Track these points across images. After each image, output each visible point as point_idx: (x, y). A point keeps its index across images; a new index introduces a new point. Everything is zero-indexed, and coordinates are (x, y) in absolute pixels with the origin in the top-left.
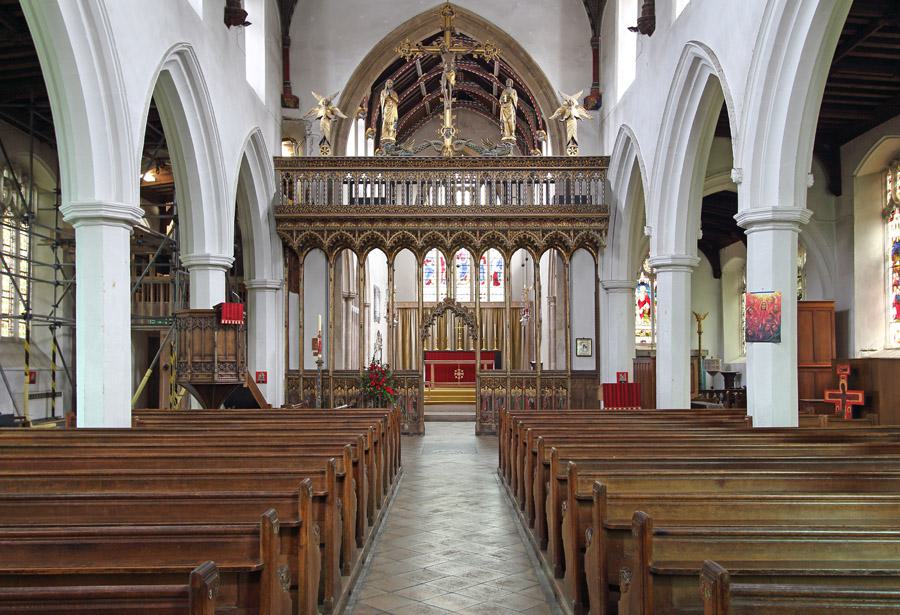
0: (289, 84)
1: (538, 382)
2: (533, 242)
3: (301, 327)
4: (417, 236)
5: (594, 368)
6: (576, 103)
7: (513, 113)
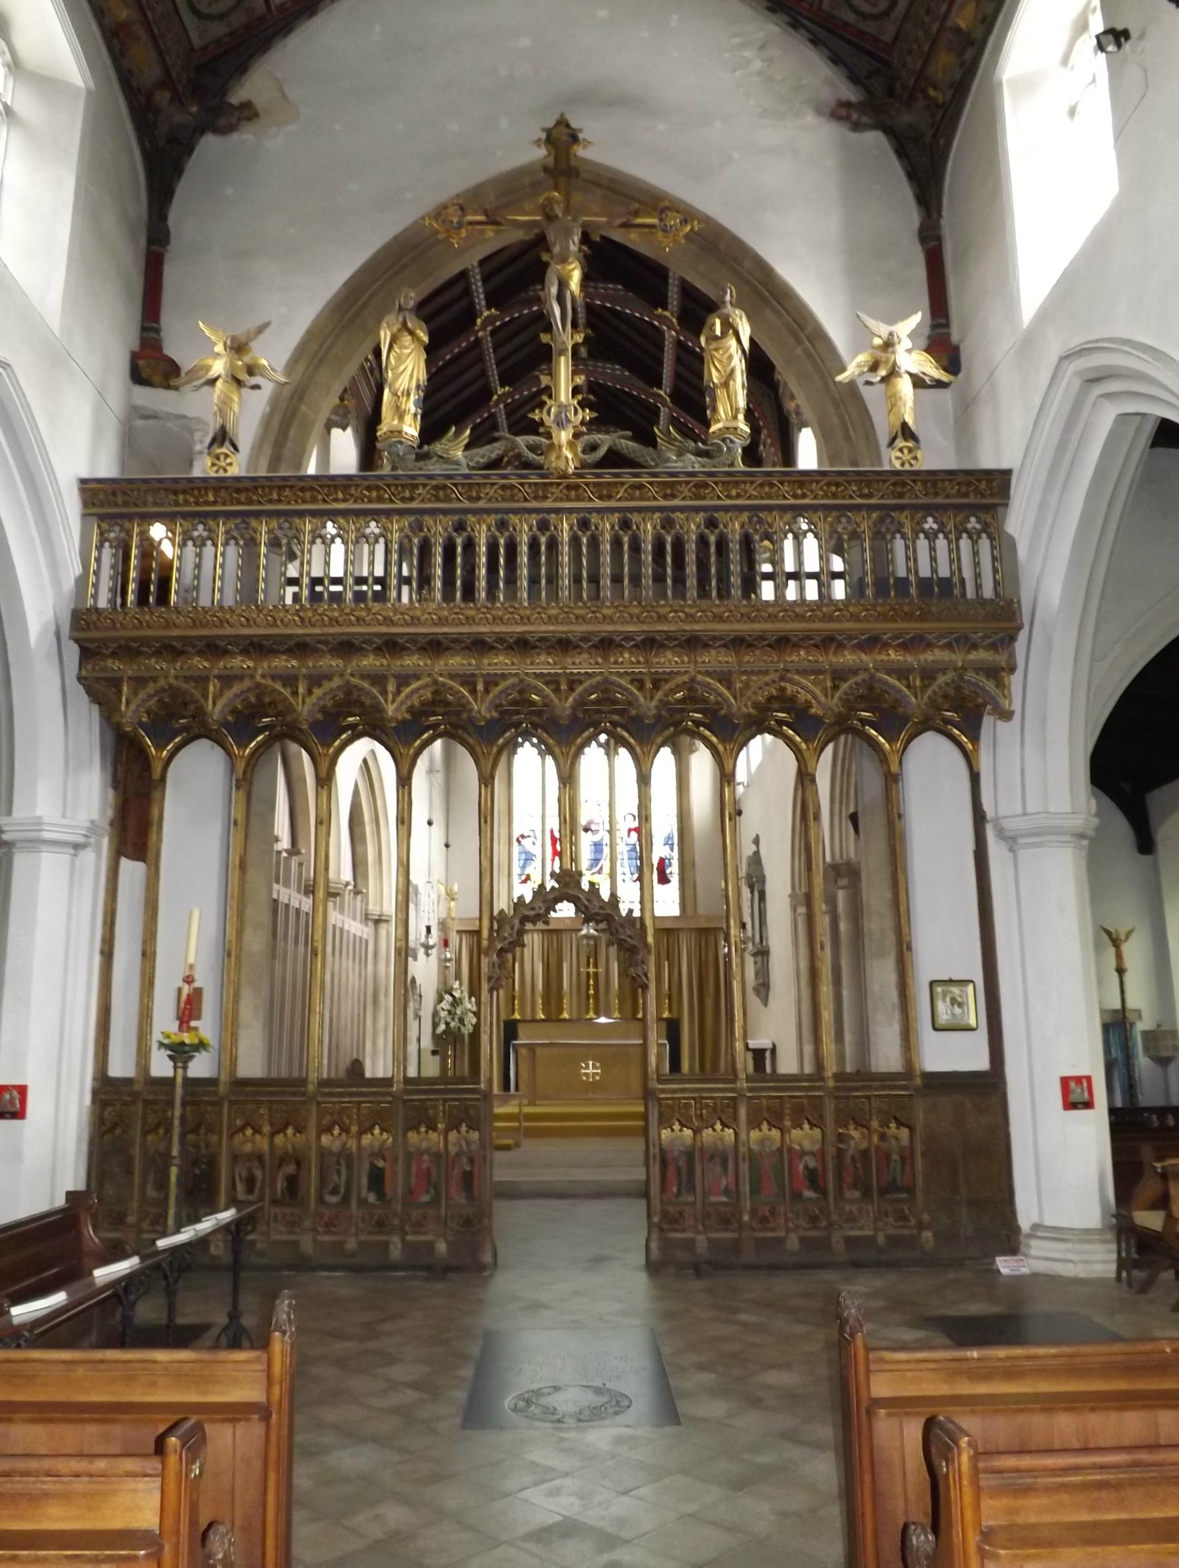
0: (157, 331)
1: (829, 1107)
2: (809, 705)
3: (148, 955)
4: (473, 691)
5: (980, 1062)
6: (906, 343)
7: (739, 365)
